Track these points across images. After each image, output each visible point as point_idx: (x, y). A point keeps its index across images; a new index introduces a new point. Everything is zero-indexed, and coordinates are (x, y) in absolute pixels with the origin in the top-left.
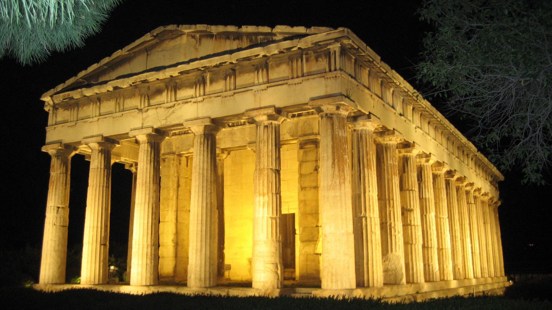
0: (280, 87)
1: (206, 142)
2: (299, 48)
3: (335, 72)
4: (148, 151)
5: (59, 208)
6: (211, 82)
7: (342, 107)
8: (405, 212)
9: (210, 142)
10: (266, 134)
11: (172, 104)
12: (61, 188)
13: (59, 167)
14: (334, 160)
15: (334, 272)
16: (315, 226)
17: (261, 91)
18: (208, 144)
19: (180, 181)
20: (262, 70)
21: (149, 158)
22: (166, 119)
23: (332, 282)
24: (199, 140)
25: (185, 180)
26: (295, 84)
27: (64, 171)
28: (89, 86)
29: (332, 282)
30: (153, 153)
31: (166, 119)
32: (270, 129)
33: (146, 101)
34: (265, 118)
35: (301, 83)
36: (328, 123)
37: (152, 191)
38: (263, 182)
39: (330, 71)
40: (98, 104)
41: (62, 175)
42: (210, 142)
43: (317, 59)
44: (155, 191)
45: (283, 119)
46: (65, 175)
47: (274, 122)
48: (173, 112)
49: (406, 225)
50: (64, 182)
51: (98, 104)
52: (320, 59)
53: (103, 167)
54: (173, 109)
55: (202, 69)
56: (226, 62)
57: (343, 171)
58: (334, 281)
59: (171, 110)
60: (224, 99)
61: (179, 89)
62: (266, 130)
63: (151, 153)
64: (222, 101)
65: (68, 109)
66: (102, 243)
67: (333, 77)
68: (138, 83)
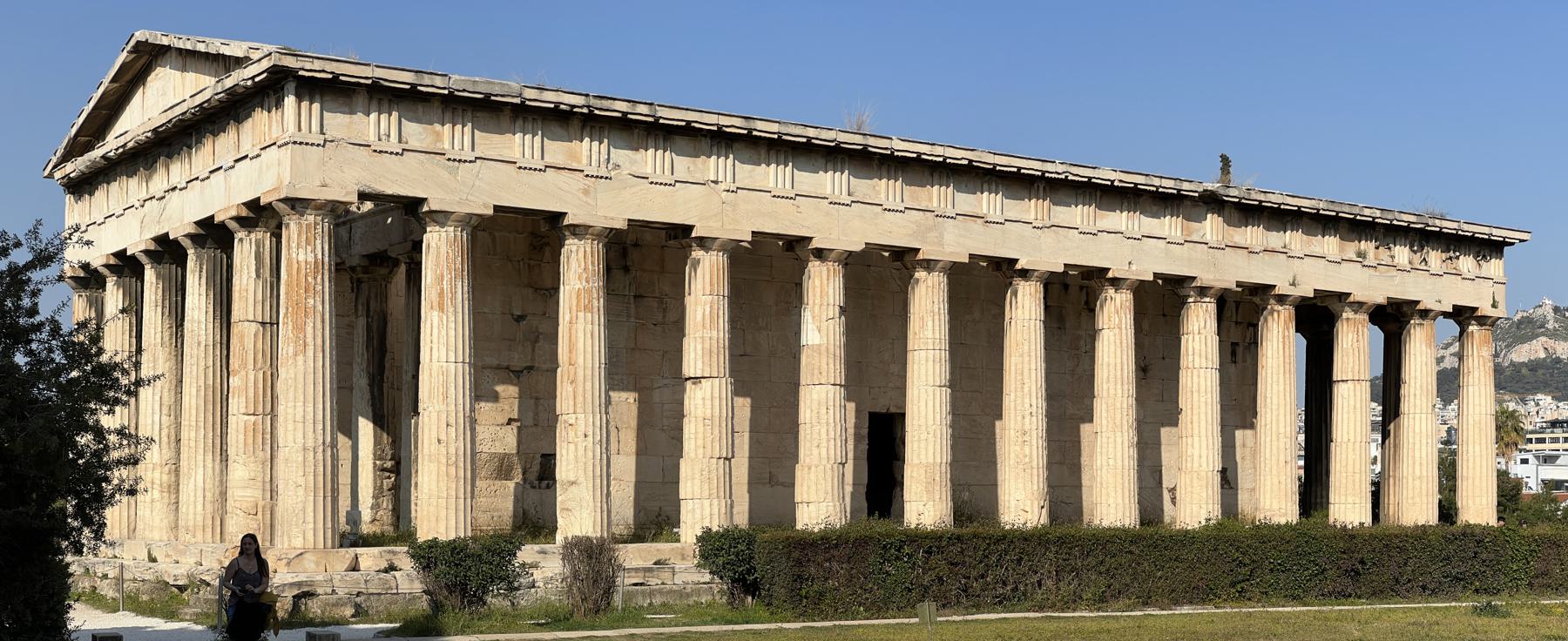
32: (246, 244)
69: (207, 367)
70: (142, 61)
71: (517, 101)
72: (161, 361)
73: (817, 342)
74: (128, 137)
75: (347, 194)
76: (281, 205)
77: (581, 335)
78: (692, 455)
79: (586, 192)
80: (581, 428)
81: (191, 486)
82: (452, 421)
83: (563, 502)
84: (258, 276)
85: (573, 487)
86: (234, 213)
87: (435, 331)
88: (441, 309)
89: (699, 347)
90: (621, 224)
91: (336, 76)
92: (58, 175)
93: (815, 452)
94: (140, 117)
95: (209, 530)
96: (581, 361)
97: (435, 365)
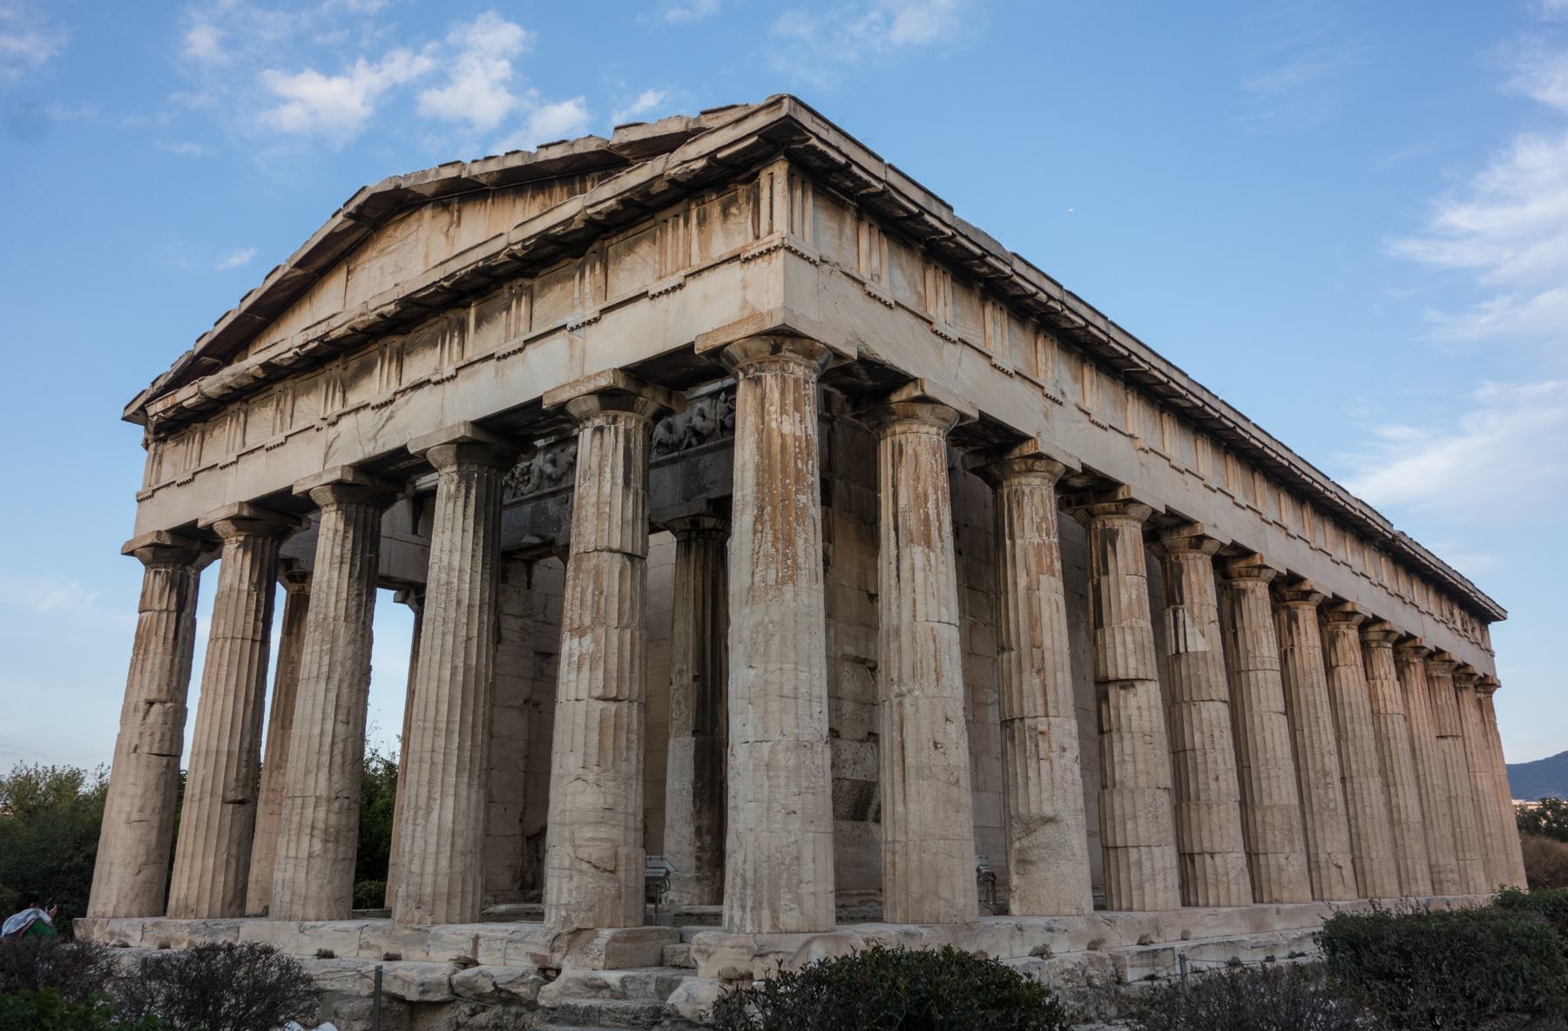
0: (630, 307)
1: (463, 491)
2: (673, 182)
3: (768, 239)
5: (151, 703)
7: (787, 345)
8: (1112, 691)
9: (473, 491)
10: (596, 450)
11: (388, 396)
12: (160, 649)
13: (156, 595)
14: (761, 509)
15: (750, 875)
18: (467, 497)
19: (504, 625)
20: (593, 269)
21: (338, 551)
22: (374, 438)
23: (743, 908)
25: (519, 622)
26: (667, 292)
27: (173, 607)
28: (212, 370)
29: (743, 908)
30: (351, 535)
31: (374, 438)
32: (609, 438)
33: (338, 395)
34: (594, 403)
35: (680, 286)
36: (750, 398)
37: (341, 642)
38: (583, 593)
39: (757, 237)
41: (164, 615)
42: (473, 491)
43: (725, 214)
44: (353, 641)
45: (652, 408)
46: (173, 616)
47: (623, 415)
48: (390, 418)
49: (1099, 732)
50: (171, 636)
52: (733, 210)
53: (245, 586)
54: (391, 408)
56: (497, 254)
57: (789, 542)
58: (749, 905)
59: (386, 412)
60: (503, 362)
61: (409, 354)
62: (597, 442)
63: (345, 538)
66: (231, 796)
67: (761, 254)
68: (311, 346)
69: (469, 639)
70: (354, 237)
71: (1008, 270)
72: (341, 642)
73: (1201, 648)
74: (335, 322)
75: (847, 343)
76: (754, 345)
77: (1045, 606)
78: (1130, 783)
79: (1046, 416)
80: (1056, 737)
81: (433, 827)
82: (950, 714)
83: (1020, 851)
84: (627, 483)
85: (1049, 830)
86: (603, 382)
87: (919, 575)
88: (928, 544)
89: (1129, 639)
90: (1077, 467)
91: (850, 162)
92: (157, 407)
93: (1213, 785)
94: (340, 304)
95: (457, 901)
96: (1047, 642)
97: (921, 626)
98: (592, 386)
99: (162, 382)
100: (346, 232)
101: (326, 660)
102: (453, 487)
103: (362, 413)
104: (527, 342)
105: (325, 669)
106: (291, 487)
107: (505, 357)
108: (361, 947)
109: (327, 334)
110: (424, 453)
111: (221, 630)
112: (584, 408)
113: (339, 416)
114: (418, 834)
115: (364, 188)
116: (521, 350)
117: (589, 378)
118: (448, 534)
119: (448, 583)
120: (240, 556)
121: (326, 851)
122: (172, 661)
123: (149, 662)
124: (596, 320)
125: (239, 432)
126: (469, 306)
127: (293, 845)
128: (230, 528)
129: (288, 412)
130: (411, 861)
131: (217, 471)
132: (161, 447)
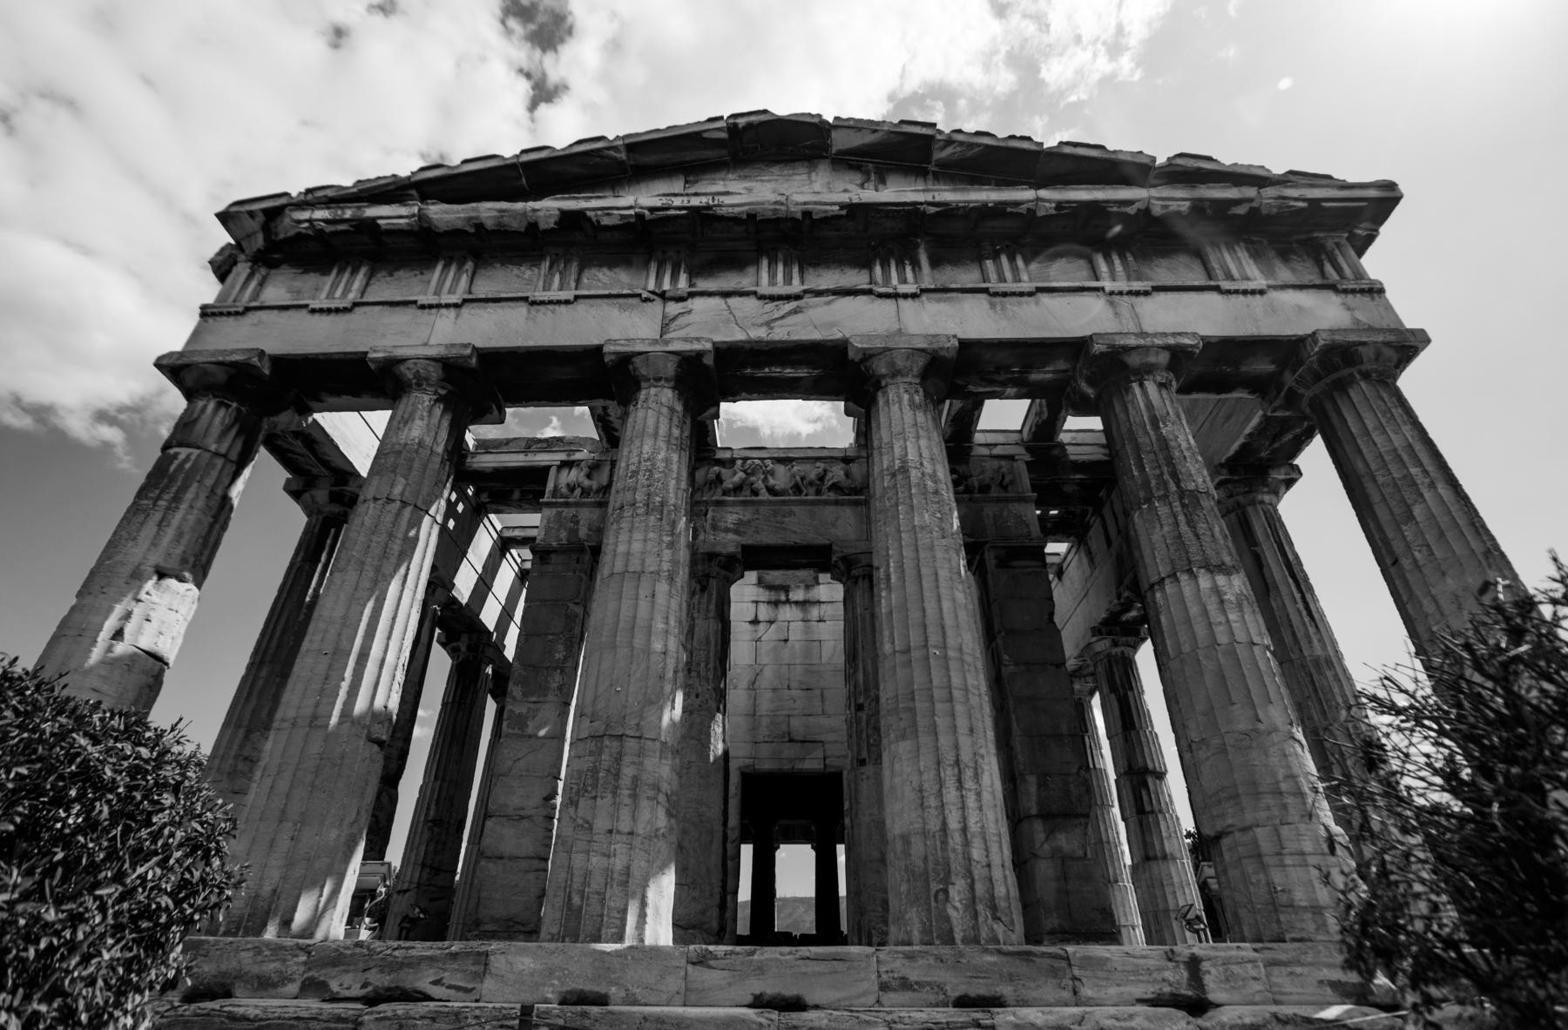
4: (672, 410)
6: (935, 263)
12: (200, 503)
16: (1074, 770)
17: (1134, 299)
24: (906, 397)
27: (234, 456)
31: (768, 324)
34: (1164, 358)
40: (469, 265)
48: (795, 312)
51: (469, 265)
53: (440, 449)
54: (793, 305)
55: (933, 210)
56: (1017, 204)
60: (998, 299)
64: (993, 306)
65: (325, 272)
68: (672, 212)
74: (727, 200)
98: (1171, 341)
99: (330, 193)
100: (718, 143)
101: (667, 554)
102: (917, 398)
103: (734, 302)
104: (1040, 290)
105: (666, 566)
106: (599, 348)
107: (1005, 294)
108: (884, 987)
109: (709, 207)
110: (868, 356)
111: (398, 490)
112: (1152, 359)
113: (692, 295)
114: (971, 802)
115: (765, 112)
116: (1030, 294)
117: (1165, 335)
118: (923, 442)
119: (936, 492)
120: (438, 411)
121: (671, 829)
122: (211, 526)
123: (179, 516)
124: (1146, 293)
125: (464, 279)
126: (917, 246)
127: (625, 814)
128: (435, 372)
129: (573, 277)
130: (967, 844)
131: (412, 310)
132: (263, 271)
